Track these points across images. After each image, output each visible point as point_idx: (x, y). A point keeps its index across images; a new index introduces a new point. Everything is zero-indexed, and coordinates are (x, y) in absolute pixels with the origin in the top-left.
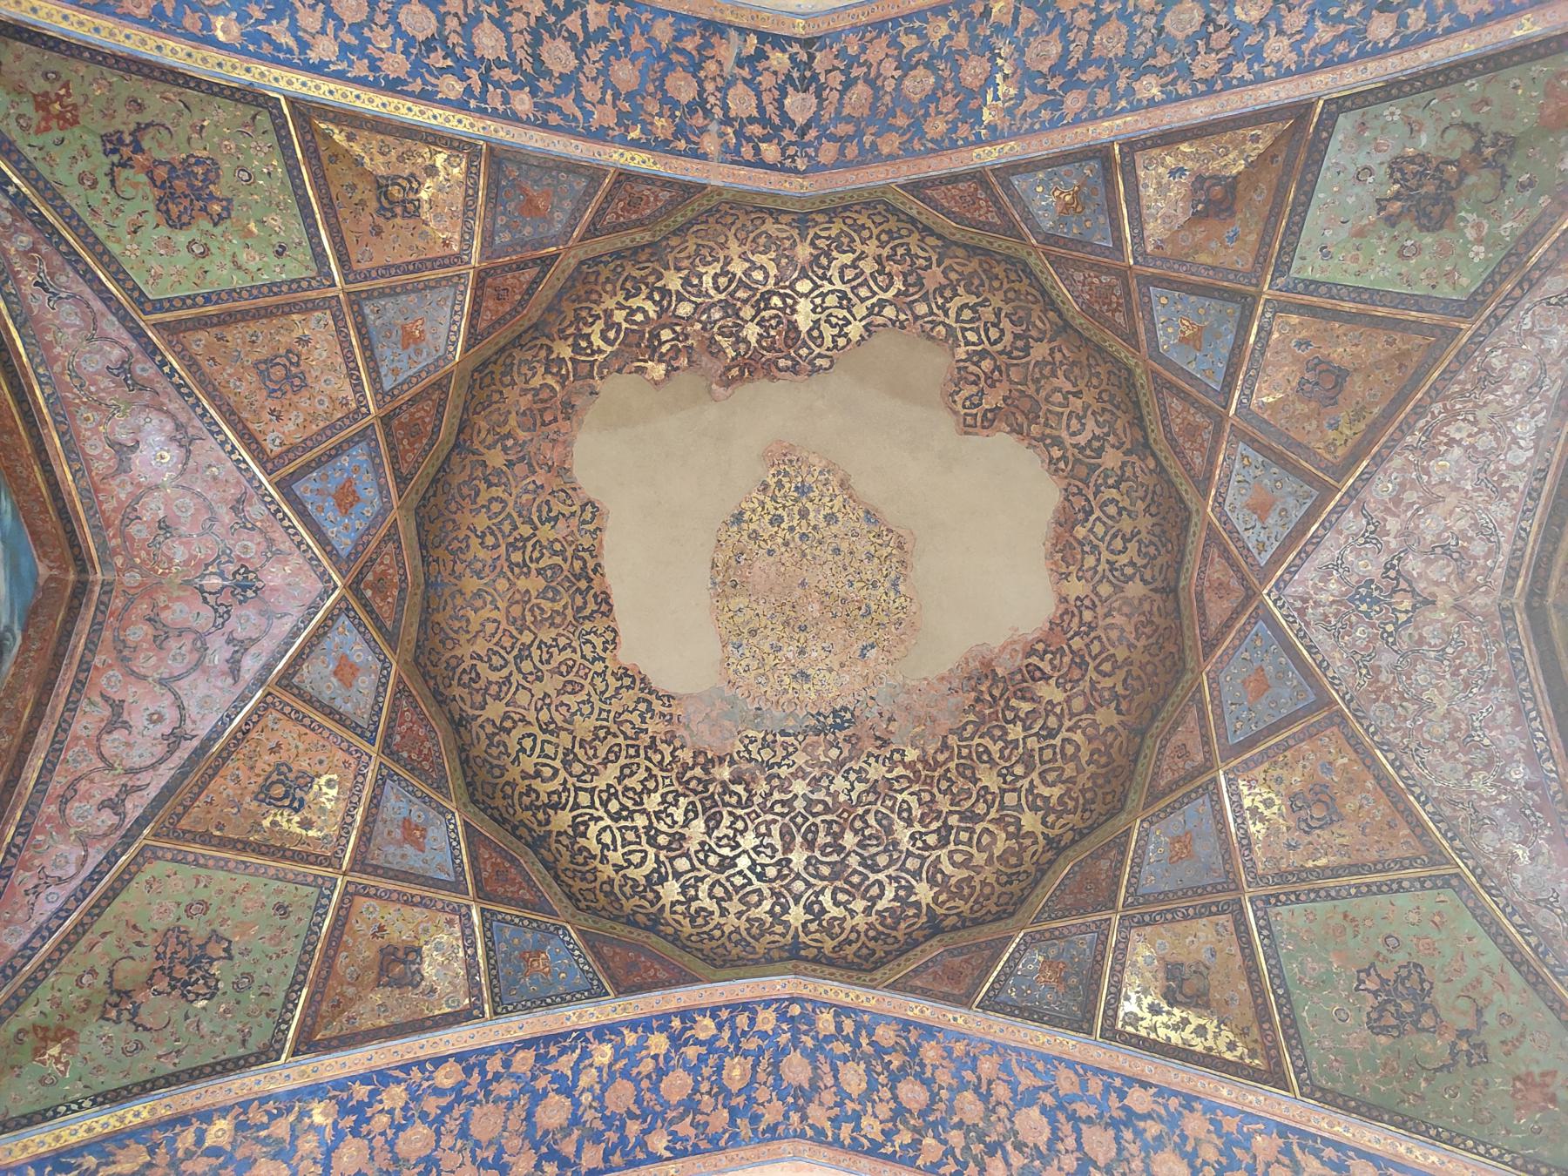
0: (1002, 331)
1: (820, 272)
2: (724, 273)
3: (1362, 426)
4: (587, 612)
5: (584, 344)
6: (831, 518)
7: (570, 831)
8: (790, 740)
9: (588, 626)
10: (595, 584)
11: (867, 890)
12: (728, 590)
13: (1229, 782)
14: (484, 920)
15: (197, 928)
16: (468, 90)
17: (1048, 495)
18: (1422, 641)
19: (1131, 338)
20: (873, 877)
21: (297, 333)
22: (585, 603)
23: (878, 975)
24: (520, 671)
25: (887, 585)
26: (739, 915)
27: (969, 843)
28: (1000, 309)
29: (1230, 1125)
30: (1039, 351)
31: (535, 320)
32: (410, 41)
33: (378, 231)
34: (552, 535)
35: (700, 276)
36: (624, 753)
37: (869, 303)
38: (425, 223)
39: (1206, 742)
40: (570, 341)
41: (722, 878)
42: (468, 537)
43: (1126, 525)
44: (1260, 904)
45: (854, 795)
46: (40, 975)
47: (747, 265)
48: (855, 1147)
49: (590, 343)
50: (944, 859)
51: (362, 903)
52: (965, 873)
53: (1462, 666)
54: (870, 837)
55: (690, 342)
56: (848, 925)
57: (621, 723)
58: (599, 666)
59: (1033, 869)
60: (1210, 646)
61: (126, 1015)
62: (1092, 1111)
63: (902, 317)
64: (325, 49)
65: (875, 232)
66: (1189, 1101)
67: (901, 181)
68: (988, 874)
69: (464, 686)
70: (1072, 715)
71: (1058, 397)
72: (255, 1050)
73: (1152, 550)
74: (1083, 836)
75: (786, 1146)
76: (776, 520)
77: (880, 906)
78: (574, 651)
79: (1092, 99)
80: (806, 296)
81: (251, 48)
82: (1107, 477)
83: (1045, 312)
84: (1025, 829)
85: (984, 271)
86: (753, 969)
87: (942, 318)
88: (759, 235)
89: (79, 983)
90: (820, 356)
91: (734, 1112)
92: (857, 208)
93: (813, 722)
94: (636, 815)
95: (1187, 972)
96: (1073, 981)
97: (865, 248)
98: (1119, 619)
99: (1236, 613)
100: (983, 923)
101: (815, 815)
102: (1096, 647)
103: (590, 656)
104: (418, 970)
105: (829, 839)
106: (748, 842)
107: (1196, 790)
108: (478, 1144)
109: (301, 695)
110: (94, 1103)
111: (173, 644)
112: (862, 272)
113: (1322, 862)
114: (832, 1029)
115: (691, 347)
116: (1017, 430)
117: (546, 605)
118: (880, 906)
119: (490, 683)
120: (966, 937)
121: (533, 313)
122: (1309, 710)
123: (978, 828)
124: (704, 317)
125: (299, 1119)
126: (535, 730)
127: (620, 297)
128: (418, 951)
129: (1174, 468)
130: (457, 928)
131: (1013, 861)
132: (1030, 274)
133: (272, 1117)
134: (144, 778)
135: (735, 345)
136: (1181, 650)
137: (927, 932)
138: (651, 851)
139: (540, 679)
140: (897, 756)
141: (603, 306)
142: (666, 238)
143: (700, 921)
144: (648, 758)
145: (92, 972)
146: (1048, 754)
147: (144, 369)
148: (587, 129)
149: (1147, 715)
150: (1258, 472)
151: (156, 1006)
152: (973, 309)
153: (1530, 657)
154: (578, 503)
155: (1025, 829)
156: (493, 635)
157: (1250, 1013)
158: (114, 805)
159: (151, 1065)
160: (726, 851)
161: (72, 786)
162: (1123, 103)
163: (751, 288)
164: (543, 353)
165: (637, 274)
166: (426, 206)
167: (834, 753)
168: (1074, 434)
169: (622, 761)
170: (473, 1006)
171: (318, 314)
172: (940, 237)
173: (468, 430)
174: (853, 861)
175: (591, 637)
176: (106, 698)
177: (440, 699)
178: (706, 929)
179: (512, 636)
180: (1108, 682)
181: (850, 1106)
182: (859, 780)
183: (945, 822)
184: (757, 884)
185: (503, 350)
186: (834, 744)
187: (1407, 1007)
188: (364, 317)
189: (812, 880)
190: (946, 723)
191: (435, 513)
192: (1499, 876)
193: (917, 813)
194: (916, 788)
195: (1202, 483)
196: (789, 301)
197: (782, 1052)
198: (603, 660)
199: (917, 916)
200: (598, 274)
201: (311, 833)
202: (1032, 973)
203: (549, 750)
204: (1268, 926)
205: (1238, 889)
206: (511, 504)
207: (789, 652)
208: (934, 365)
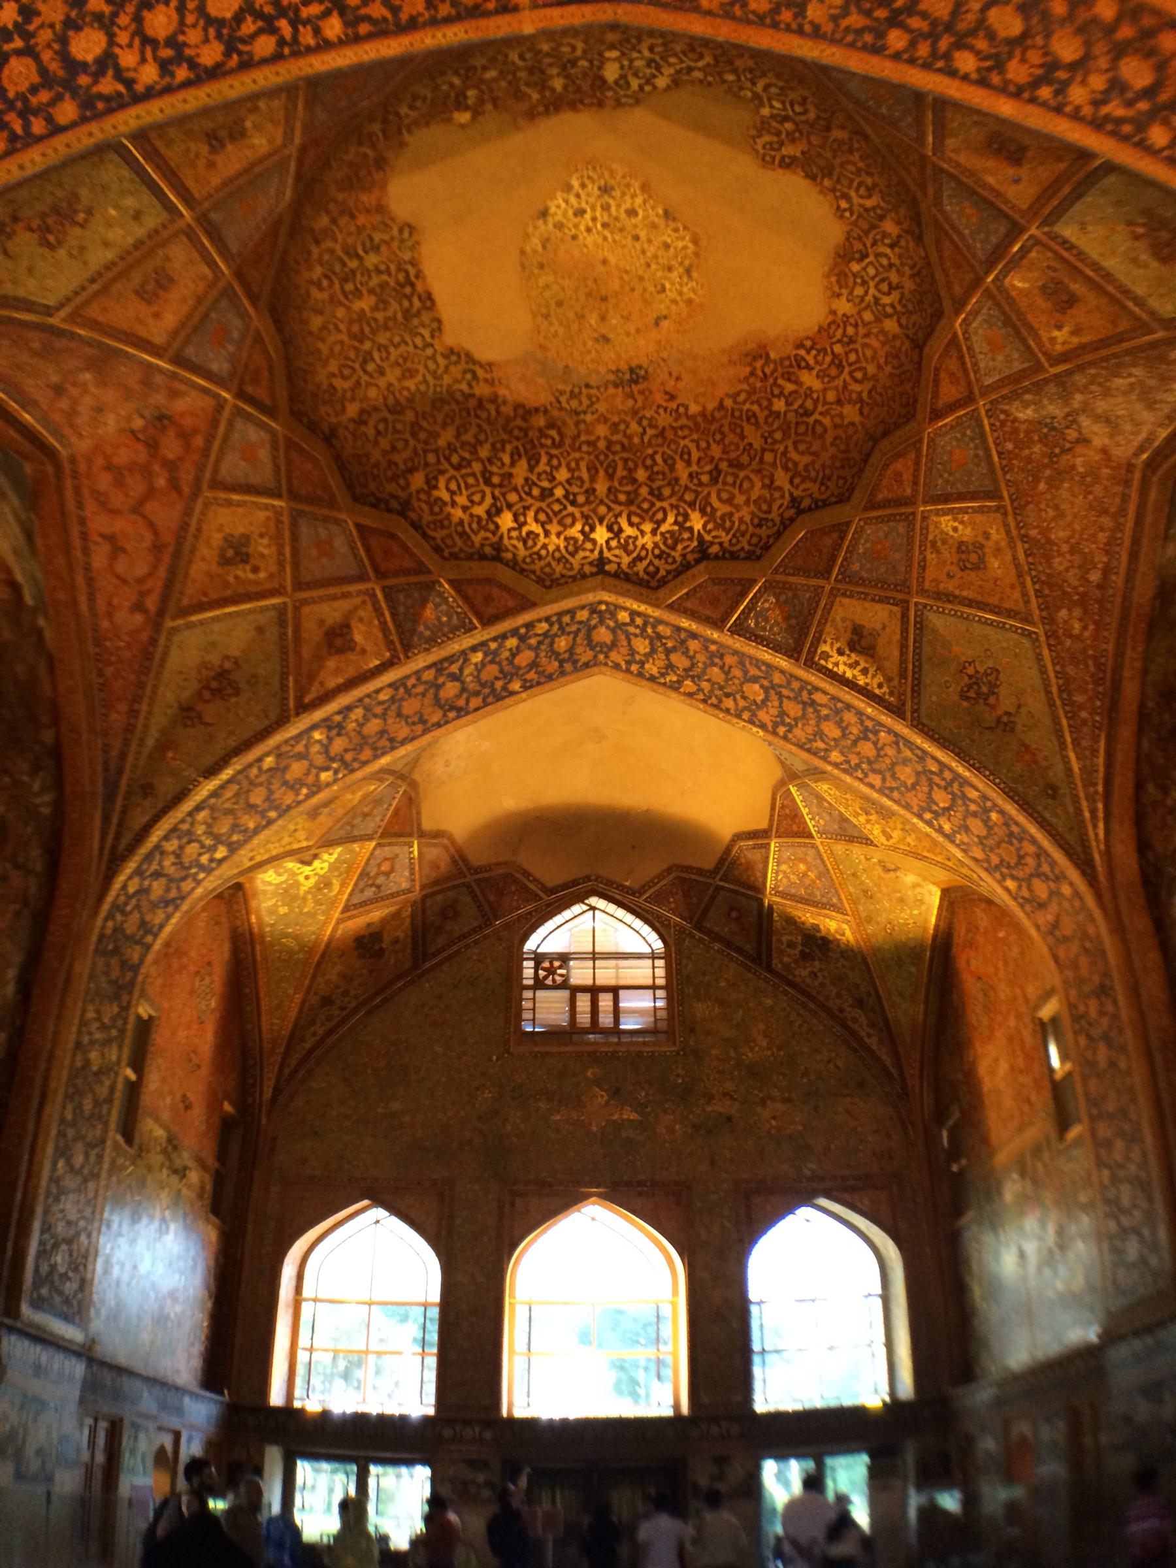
3: (1076, 340)
6: (632, 213)
8: (594, 391)
9: (416, 321)
10: (420, 288)
11: (654, 514)
14: (385, 595)
15: (214, 659)
16: (282, 42)
17: (835, 232)
18: (1073, 467)
19: (923, 187)
20: (658, 504)
23: (661, 593)
24: (365, 371)
25: (681, 270)
29: (869, 724)
32: (220, 23)
39: (915, 483)
41: (543, 505)
43: (894, 277)
45: (646, 439)
48: (640, 675)
51: (306, 610)
52: (726, 509)
53: (1091, 493)
56: (640, 542)
58: (429, 352)
59: (778, 520)
60: (937, 415)
62: (792, 695)
64: (149, 74)
66: (849, 707)
68: (745, 513)
74: (817, 507)
75: (596, 669)
77: (663, 528)
78: (407, 344)
79: (913, 44)
81: (88, 113)
84: (777, 483)
91: (561, 662)
93: (612, 377)
94: (474, 464)
95: (865, 632)
100: (737, 558)
101: (614, 453)
102: (853, 357)
104: (353, 640)
105: (625, 473)
106: (562, 475)
111: (129, 481)
113: (964, 593)
114: (628, 620)
117: (380, 316)
119: (345, 391)
122: (989, 496)
123: (742, 474)
128: (348, 626)
130: (369, 606)
131: (764, 507)
134: (149, 584)
135: (541, 92)
137: (696, 556)
138: (488, 490)
140: (681, 410)
143: (530, 543)
144: (477, 416)
146: (802, 429)
147: (60, 343)
148: (398, 24)
153: (1132, 508)
155: (777, 483)
157: (896, 670)
158: (139, 607)
160: (546, 484)
161: (110, 604)
162: (940, 64)
167: (630, 402)
169: (458, 422)
170: (393, 656)
174: (644, 491)
175: (422, 331)
176: (102, 536)
177: (312, 427)
178: (536, 549)
179: (355, 348)
180: (856, 387)
181: (638, 657)
182: (651, 426)
183: (716, 467)
184: (570, 509)
187: (984, 689)
192: (1058, 638)
194: (695, 436)
195: (959, 306)
197: (591, 629)
199: (690, 539)
201: (262, 575)
202: (768, 610)
203: (399, 426)
204: (921, 623)
207: (593, 319)
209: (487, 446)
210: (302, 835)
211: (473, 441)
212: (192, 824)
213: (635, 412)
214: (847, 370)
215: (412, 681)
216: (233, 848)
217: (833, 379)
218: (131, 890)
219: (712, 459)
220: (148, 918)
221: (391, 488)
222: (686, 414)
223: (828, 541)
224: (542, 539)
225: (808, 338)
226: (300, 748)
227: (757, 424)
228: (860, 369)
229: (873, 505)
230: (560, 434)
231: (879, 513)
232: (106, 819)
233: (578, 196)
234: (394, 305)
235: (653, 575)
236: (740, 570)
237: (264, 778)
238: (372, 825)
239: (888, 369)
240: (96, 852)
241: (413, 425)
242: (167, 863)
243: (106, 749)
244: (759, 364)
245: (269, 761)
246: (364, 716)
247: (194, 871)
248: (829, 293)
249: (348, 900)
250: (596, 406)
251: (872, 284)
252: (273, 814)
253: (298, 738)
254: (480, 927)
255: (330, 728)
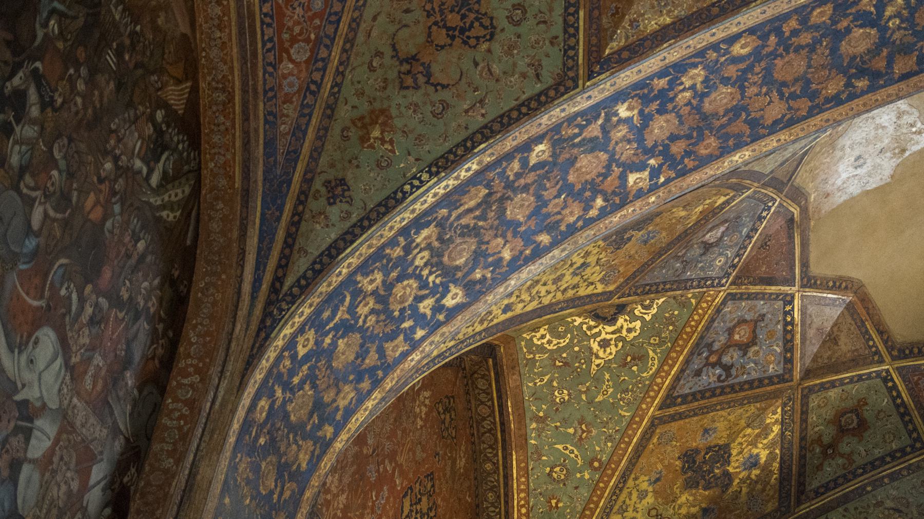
46: (339, 80)
61: (421, 79)
72: (551, 82)
89: (372, 69)
108: (784, 84)
110: (431, 175)
125: (607, 120)
133: (582, 128)
145: (379, 54)
151: (447, 63)
159: (462, 121)
210: (594, 273)
212: (407, 250)
215: (794, 23)
216: (475, 291)
218: (302, 351)
220: (327, 398)
226: (594, 130)
232: (266, 236)
237: (531, 178)
238: (720, 262)
240: (247, 287)
242: (362, 310)
243: (272, 119)
245: (541, 151)
246: (706, 81)
247: (406, 325)
249: (673, 387)
252: (544, 239)
253: (590, 115)
254: (903, 451)
255: (646, 100)
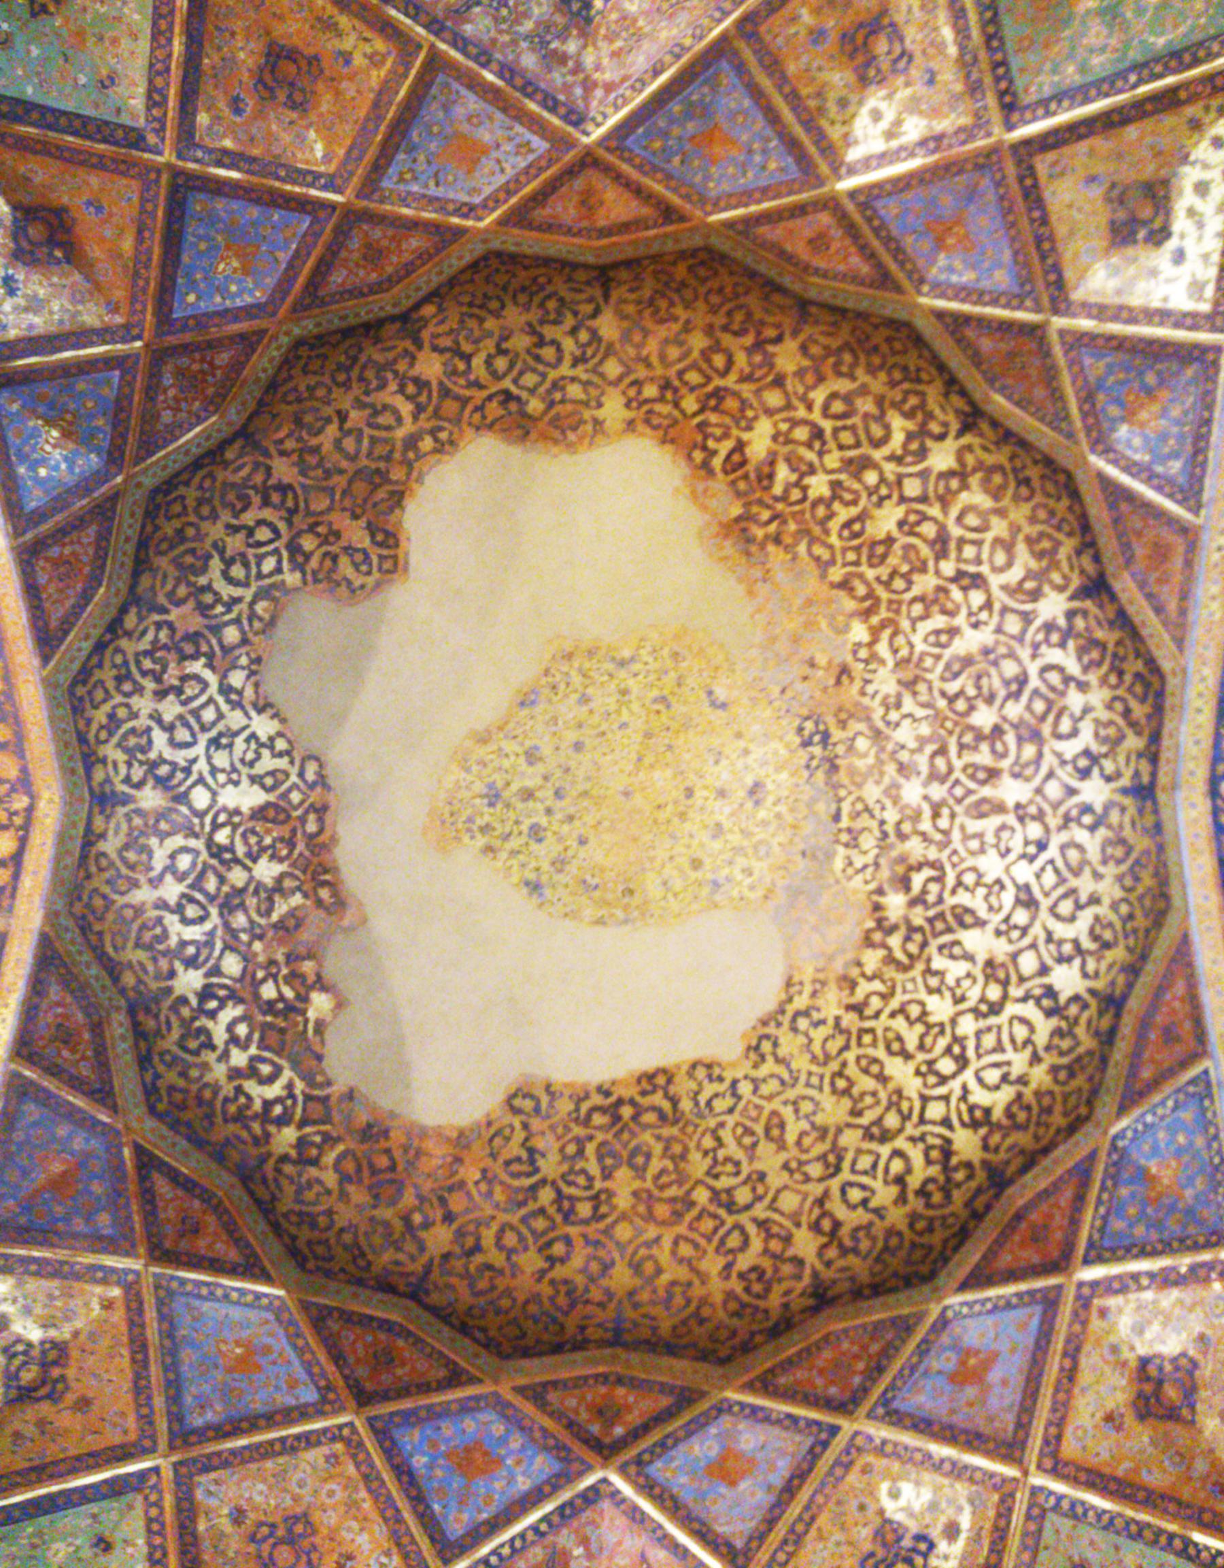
0: (260, 523)
1: (180, 775)
2: (179, 909)
4: (666, 1106)
5: (278, 1110)
6: (532, 756)
7: (983, 1131)
8: (846, 807)
9: (686, 1105)
10: (627, 1093)
11: (1053, 689)
12: (637, 900)
13: (852, 171)
19: (249, 342)
20: (1034, 682)
21: (225, 1524)
22: (653, 1108)
24: (748, 1207)
26: (1097, 876)
27: (978, 543)
28: (228, 526)
30: (283, 470)
31: (234, 1180)
33: (84, 1403)
34: (554, 1157)
35: (184, 944)
36: (870, 1051)
37: (224, 707)
38: (76, 1334)
39: (800, 210)
40: (272, 1129)
41: (1045, 903)
42: (552, 1282)
43: (521, 342)
44: (1015, 117)
45: (921, 713)
47: (169, 878)
49: (278, 1100)
50: (1003, 578)
54: (979, 687)
55: (280, 958)
57: (827, 1058)
58: (745, 1088)
59: (1007, 450)
60: (668, 213)
63: (244, 661)
65: (119, 699)
67: (36, 662)
68: (1020, 513)
69: (768, 1290)
70: (789, 406)
71: (349, 444)
73: (551, 305)
76: (536, 833)
77: (1073, 668)
80: (214, 794)
82: (455, 372)
83: (226, 464)
85: (172, 547)
86: (1170, 853)
87: (244, 606)
88: (124, 861)
90: (301, 775)
92: (81, 724)
94: (960, 1032)
95: (1121, 215)
96: (1150, 379)
97: (145, 712)
98: (652, 346)
99: (618, 177)
102: (693, 377)
103: (729, 1101)
107: (869, 220)
109: (760, 1537)
112: (181, 717)
115: (289, 958)
116: (398, 498)
118: (1073, 668)
119: (766, 1251)
120: (1108, 542)
121: (221, 1182)
124: (244, 937)
126: (835, 1184)
127: (210, 1057)
129: (428, 278)
132: (168, 485)
136: (682, 255)
138: (1011, 1009)
139: (762, 1176)
140: (863, 653)
141: (223, 1080)
142: (123, 991)
143: (1108, 935)
144: (877, 1015)
149: (777, 298)
150: (422, 158)
152: (229, 563)
154: (508, 1118)
156: (696, 1246)
160: (1008, 897)
163: (203, 873)
164: (288, 1169)
165: (175, 1035)
166: (52, 1333)
167: (862, 744)
168: (399, 420)
169: (880, 1053)
171: (199, 1494)
172: (123, 610)
173: (395, 1279)
174: (1014, 710)
179: (699, 1218)
180: (741, 359)
182: (898, 706)
183: (954, 580)
184: (1053, 851)
185: (276, 1227)
186: (851, 749)
188: (209, 1427)
189: (1044, 771)
190: (812, 584)
191: (513, 1331)
193: (939, 621)
195: (446, 236)
196: (222, 818)
198: (735, 1083)
200: (172, 1089)
202: (1146, 439)
203: (865, 1162)
205: (995, 150)
206: (504, 1217)
207: (722, 812)
208: (314, 619)
209: (933, 1002)
211: (919, 1028)
213: (877, 735)
214: (718, 382)
217: (744, 404)
219: (940, 589)
221: (958, 1197)
222: (871, 644)
223: (986, 344)
224: (1103, 910)
225: (689, 457)
227: (862, 517)
228: (708, 360)
229: (884, 280)
230: (919, 867)
231: (887, 259)
233: (507, 837)
234: (647, 1137)
235: (1147, 686)
236: (1097, 510)
239: (679, 311)
241: (868, 1135)
244: (760, 533)
248: (599, 439)
250: (871, 802)
251: (553, 374)
